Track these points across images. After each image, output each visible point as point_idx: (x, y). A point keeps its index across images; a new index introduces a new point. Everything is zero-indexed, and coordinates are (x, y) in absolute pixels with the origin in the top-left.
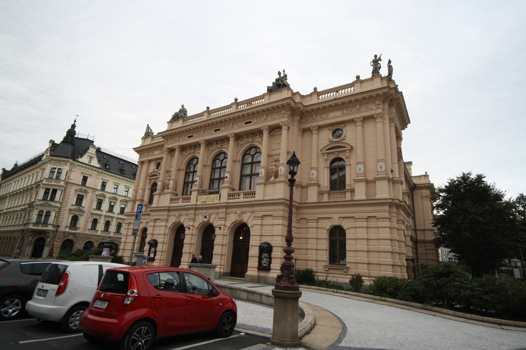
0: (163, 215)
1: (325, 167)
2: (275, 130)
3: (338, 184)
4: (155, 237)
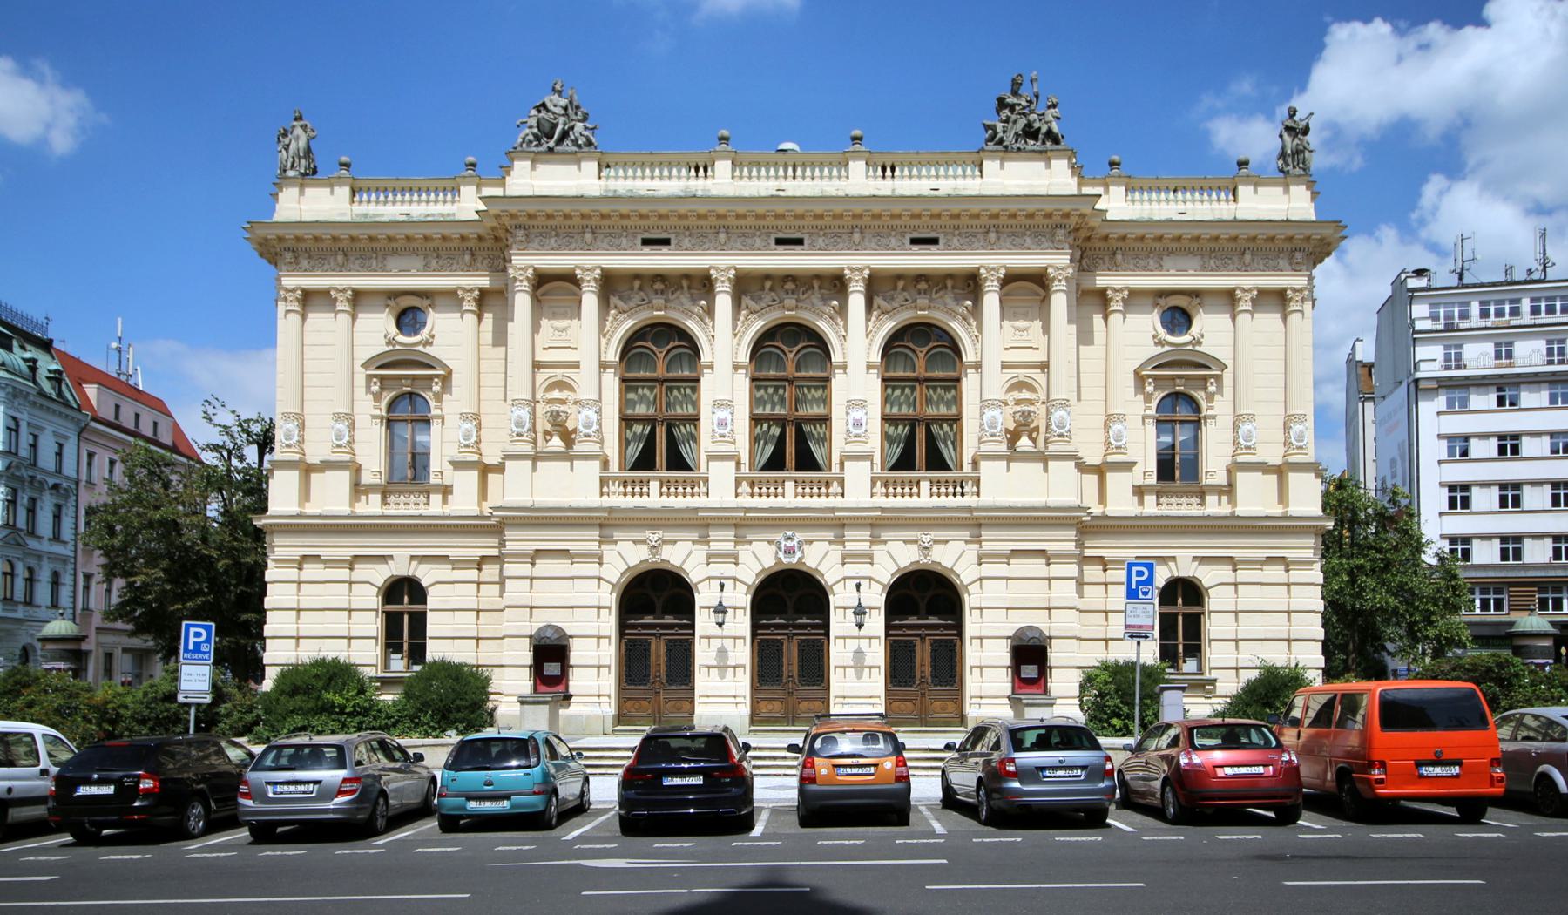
1: (374, 417)
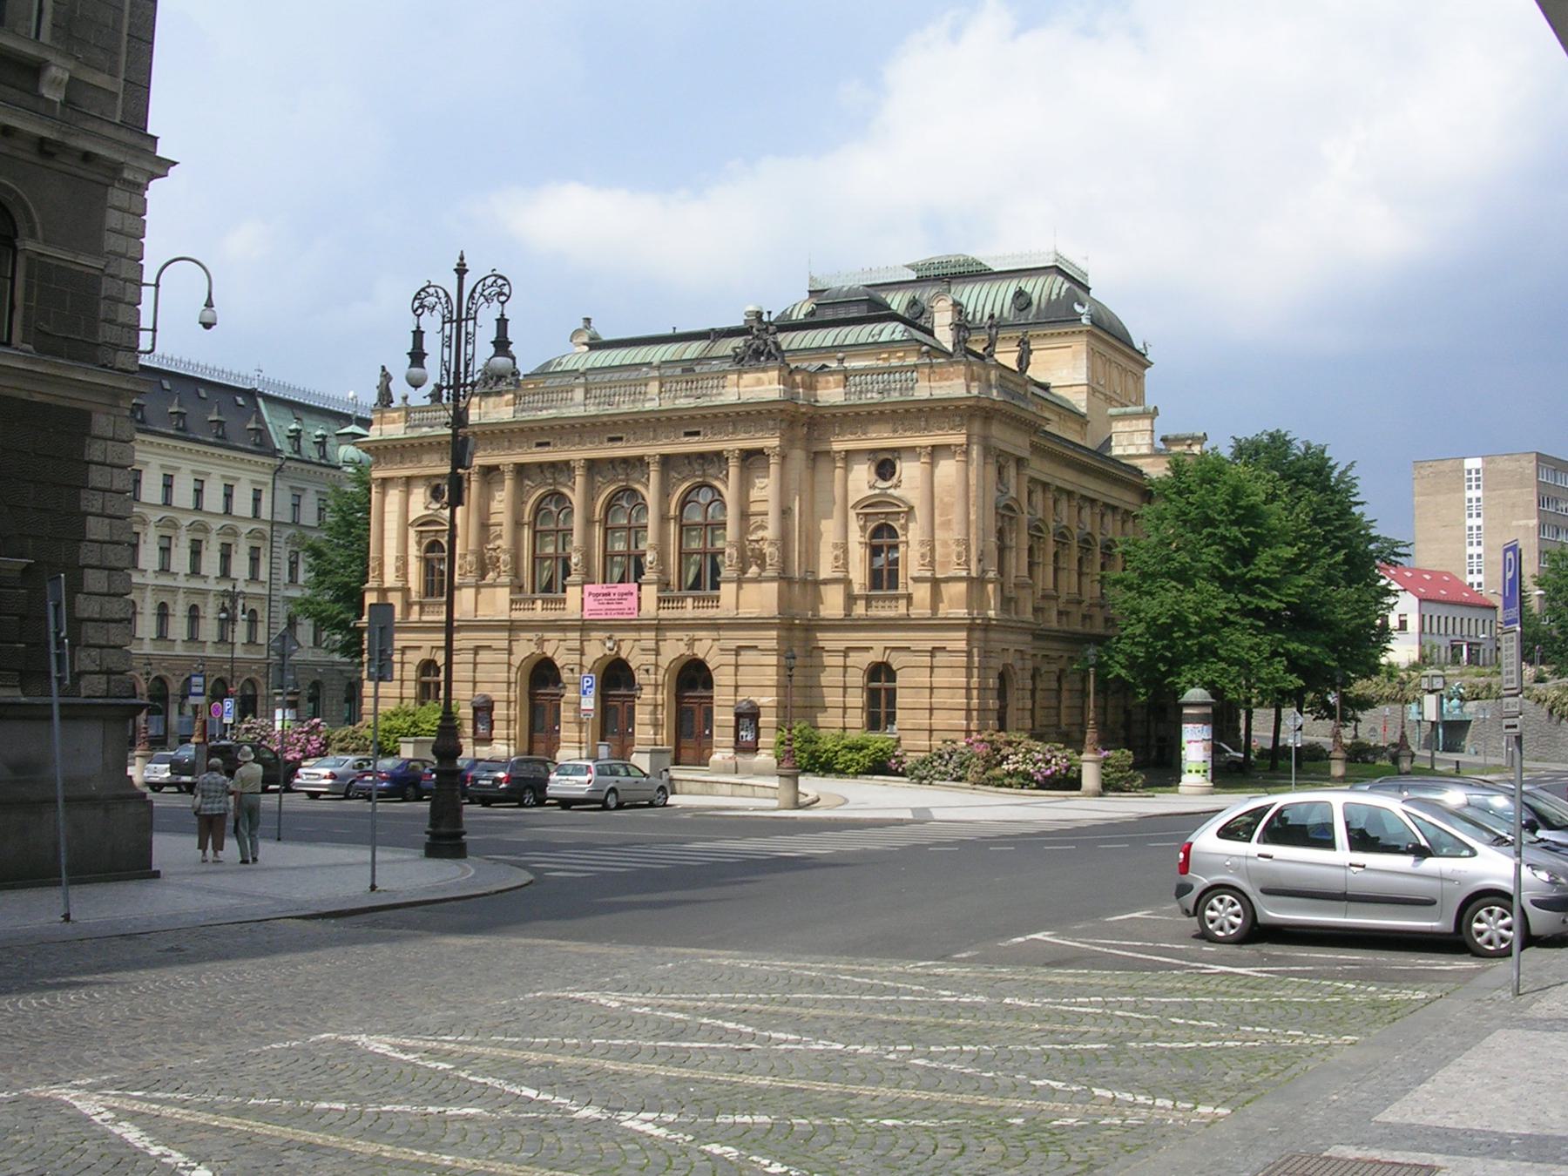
0: (500, 639)
2: (752, 458)
3: (884, 578)
4: (484, 689)
